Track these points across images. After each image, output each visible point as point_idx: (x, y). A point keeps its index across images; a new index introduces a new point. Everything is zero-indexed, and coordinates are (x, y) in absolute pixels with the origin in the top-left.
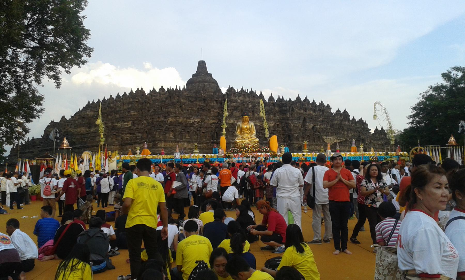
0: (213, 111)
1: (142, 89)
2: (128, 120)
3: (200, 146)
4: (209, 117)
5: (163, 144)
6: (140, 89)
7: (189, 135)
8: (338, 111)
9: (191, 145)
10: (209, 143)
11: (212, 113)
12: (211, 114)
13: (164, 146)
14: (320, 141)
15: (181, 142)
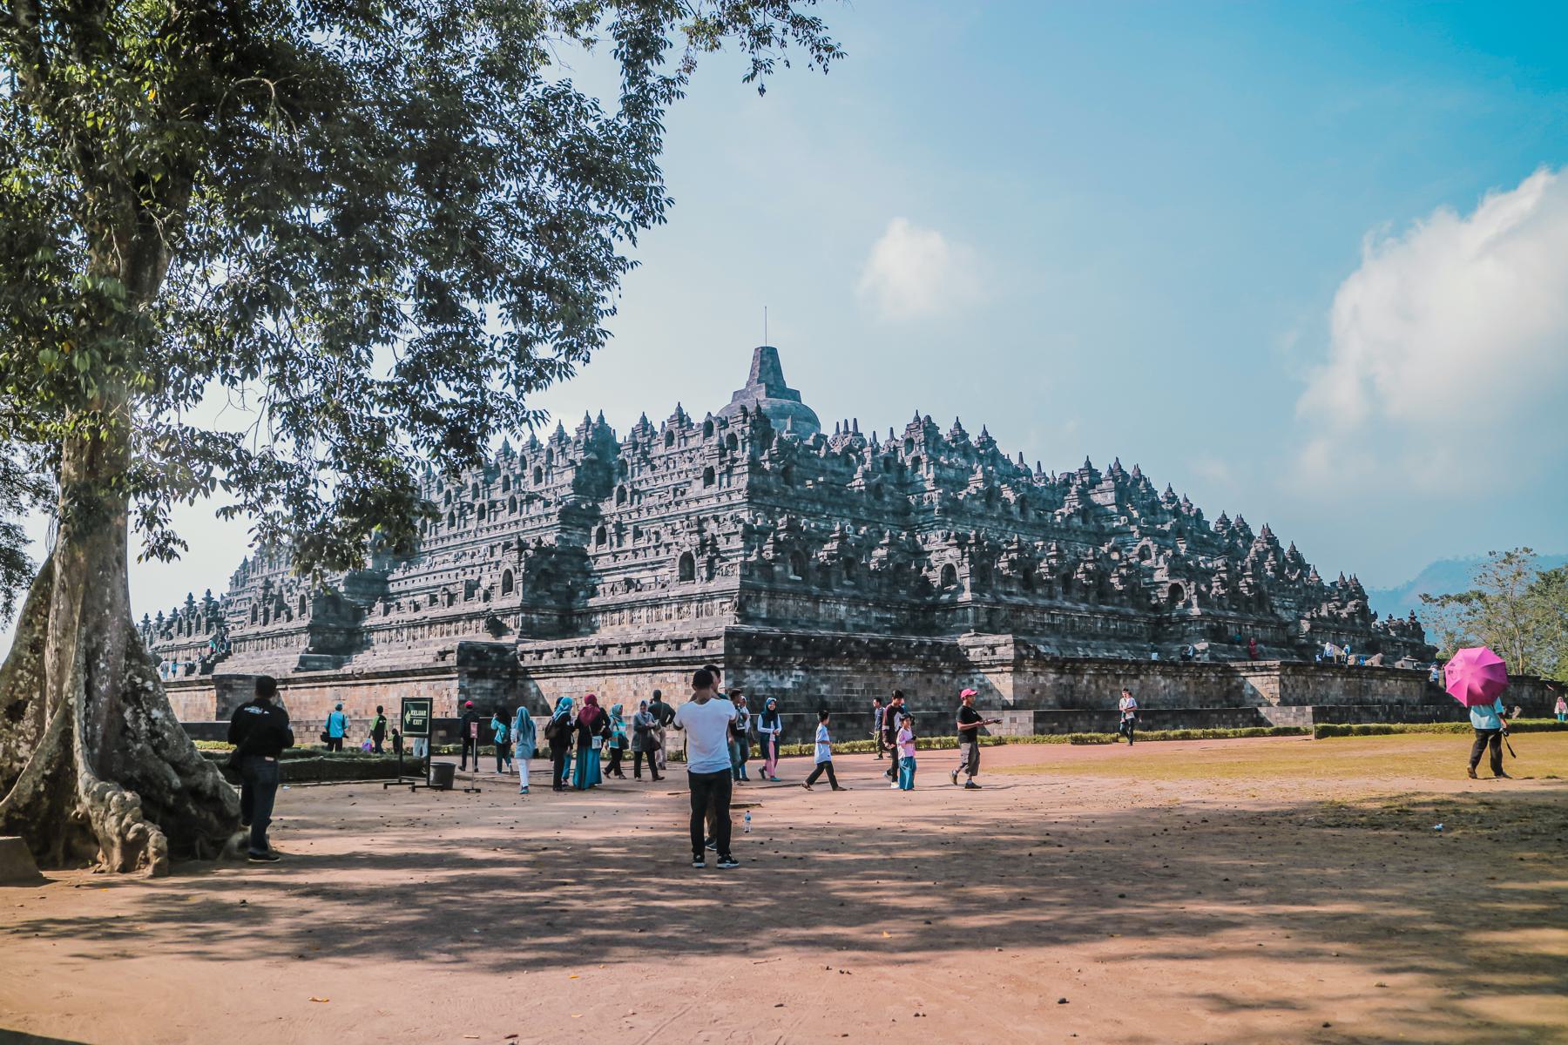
0: (891, 494)
1: (601, 418)
2: (571, 524)
3: (891, 619)
4: (879, 514)
5: (764, 605)
6: (594, 420)
7: (848, 573)
8: (1224, 521)
9: (861, 612)
10: (920, 605)
11: (887, 499)
12: (884, 503)
13: (769, 612)
14: (1264, 610)
15: (827, 597)
